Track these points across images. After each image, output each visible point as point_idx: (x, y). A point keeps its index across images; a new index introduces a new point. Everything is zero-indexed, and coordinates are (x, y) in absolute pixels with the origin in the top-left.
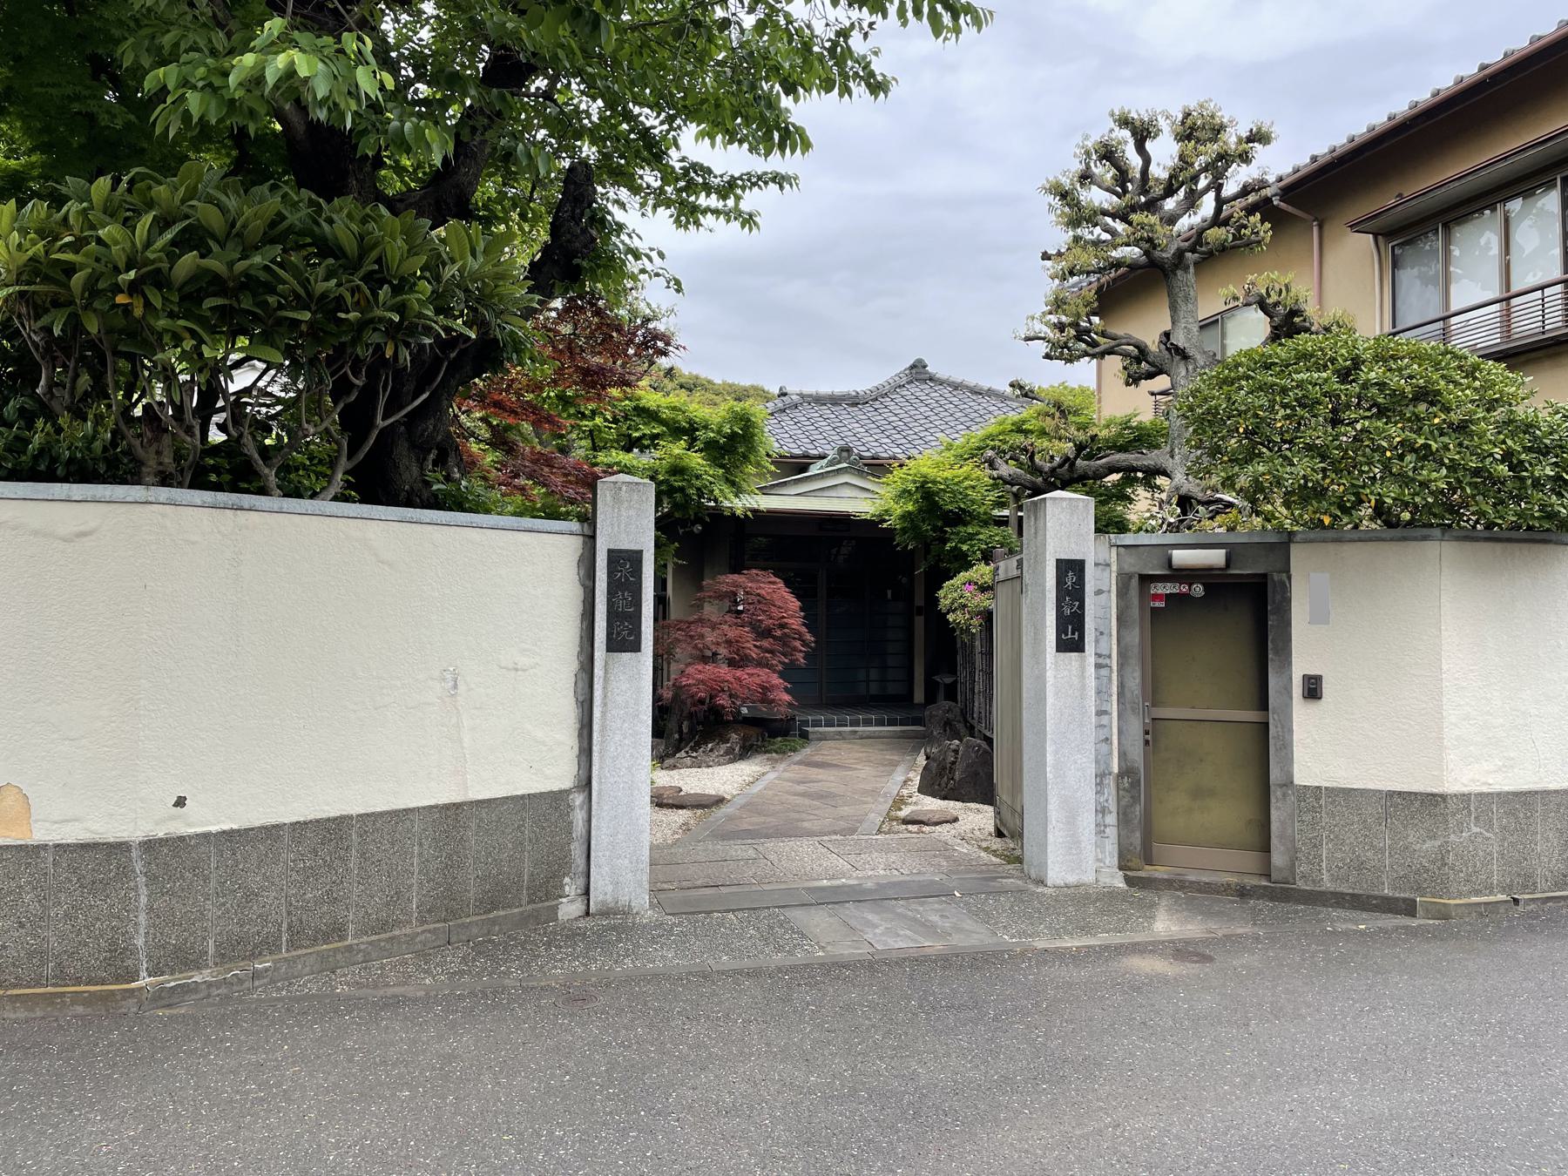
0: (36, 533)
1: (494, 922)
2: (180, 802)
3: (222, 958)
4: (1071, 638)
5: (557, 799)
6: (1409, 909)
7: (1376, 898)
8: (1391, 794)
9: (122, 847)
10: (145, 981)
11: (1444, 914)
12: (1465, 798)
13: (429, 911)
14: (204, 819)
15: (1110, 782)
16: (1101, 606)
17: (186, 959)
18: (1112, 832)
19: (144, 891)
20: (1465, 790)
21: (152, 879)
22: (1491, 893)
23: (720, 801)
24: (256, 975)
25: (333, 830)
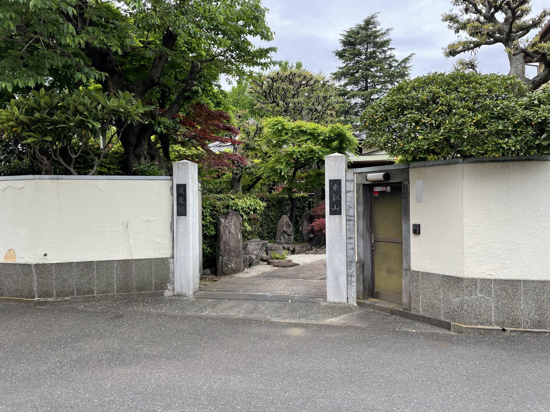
0: (14, 188)
1: (141, 294)
2: (45, 255)
3: (58, 295)
4: (336, 210)
5: (164, 261)
6: (448, 326)
7: (436, 320)
8: (444, 276)
9: (29, 265)
10: (36, 299)
11: (460, 331)
12: (474, 281)
13: (120, 289)
14: (52, 259)
15: (354, 265)
16: (350, 197)
17: (48, 294)
18: (354, 284)
19: (35, 277)
20: (476, 277)
21: (37, 274)
22: (491, 324)
23: (298, 265)
24: (66, 301)
25: (89, 264)
